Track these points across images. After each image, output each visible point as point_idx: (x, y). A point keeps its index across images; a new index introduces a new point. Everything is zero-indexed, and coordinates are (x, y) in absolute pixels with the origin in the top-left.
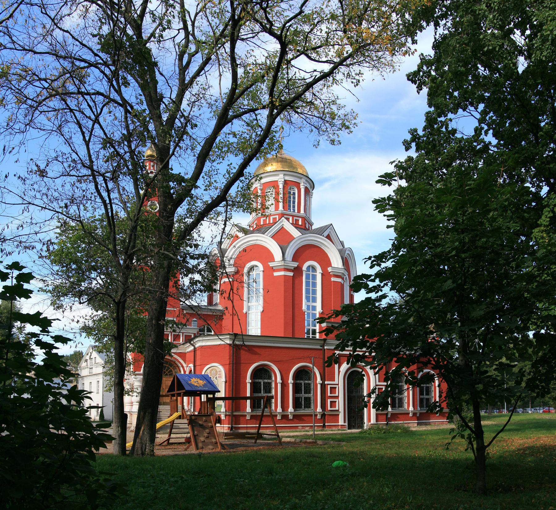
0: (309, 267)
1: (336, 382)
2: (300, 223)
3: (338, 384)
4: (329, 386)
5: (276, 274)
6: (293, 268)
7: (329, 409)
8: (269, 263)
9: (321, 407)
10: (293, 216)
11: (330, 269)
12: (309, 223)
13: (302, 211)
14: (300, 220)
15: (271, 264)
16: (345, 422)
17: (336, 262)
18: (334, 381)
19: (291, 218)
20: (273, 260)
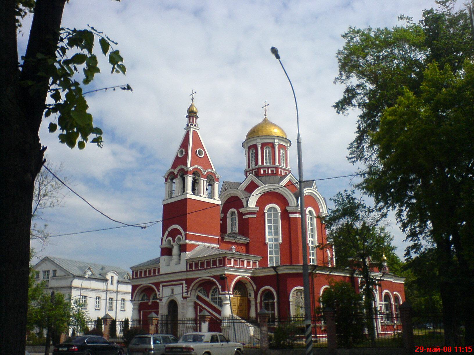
0: (271, 208)
5: (244, 217)
8: (240, 210)
14: (275, 169)
15: (241, 210)
20: (243, 207)
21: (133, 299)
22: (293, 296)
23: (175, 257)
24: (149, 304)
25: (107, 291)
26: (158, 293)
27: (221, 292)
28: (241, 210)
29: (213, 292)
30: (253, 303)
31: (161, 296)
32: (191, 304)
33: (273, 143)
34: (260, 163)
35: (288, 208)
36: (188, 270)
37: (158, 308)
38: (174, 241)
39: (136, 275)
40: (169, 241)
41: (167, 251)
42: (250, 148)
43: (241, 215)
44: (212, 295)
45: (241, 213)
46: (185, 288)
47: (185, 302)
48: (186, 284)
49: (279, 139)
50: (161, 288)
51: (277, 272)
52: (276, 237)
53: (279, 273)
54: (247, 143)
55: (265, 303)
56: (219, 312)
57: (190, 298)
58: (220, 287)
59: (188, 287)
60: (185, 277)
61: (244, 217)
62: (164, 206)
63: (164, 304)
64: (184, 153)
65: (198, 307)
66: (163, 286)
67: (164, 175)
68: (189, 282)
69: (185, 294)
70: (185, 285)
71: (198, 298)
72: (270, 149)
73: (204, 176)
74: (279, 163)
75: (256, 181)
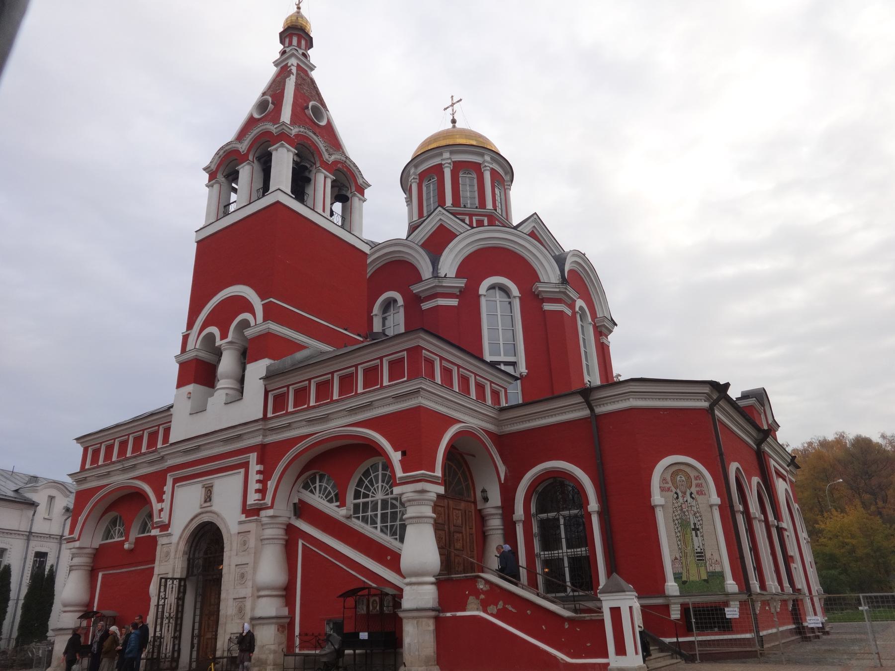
0: (492, 287)
5: (426, 306)
6: (457, 291)
10: (471, 216)
15: (416, 289)
20: (418, 279)
21: (76, 535)
22: (662, 489)
23: (224, 384)
24: (126, 546)
25: (30, 535)
26: (156, 506)
27: (399, 473)
28: (416, 289)
29: (360, 483)
30: (495, 523)
31: (165, 517)
32: (275, 532)
33: (480, 164)
35: (541, 288)
36: (270, 415)
37: (153, 561)
38: (224, 336)
39: (95, 459)
40: (211, 337)
41: (198, 372)
42: (422, 176)
43: (413, 302)
44: (357, 495)
46: (254, 477)
47: (252, 527)
48: (260, 461)
49: (492, 158)
50: (168, 488)
51: (592, 410)
53: (600, 410)
54: (416, 167)
55: (542, 524)
56: (392, 560)
57: (270, 512)
58: (396, 457)
59: (266, 475)
60: (257, 440)
61: (426, 306)
62: (198, 242)
63: (175, 539)
64: (271, 106)
65: (300, 542)
66: (176, 481)
67: (206, 163)
68: (268, 455)
69: (253, 498)
70: (254, 467)
71: (302, 510)
72: (475, 176)
73: (326, 165)
75: (452, 223)
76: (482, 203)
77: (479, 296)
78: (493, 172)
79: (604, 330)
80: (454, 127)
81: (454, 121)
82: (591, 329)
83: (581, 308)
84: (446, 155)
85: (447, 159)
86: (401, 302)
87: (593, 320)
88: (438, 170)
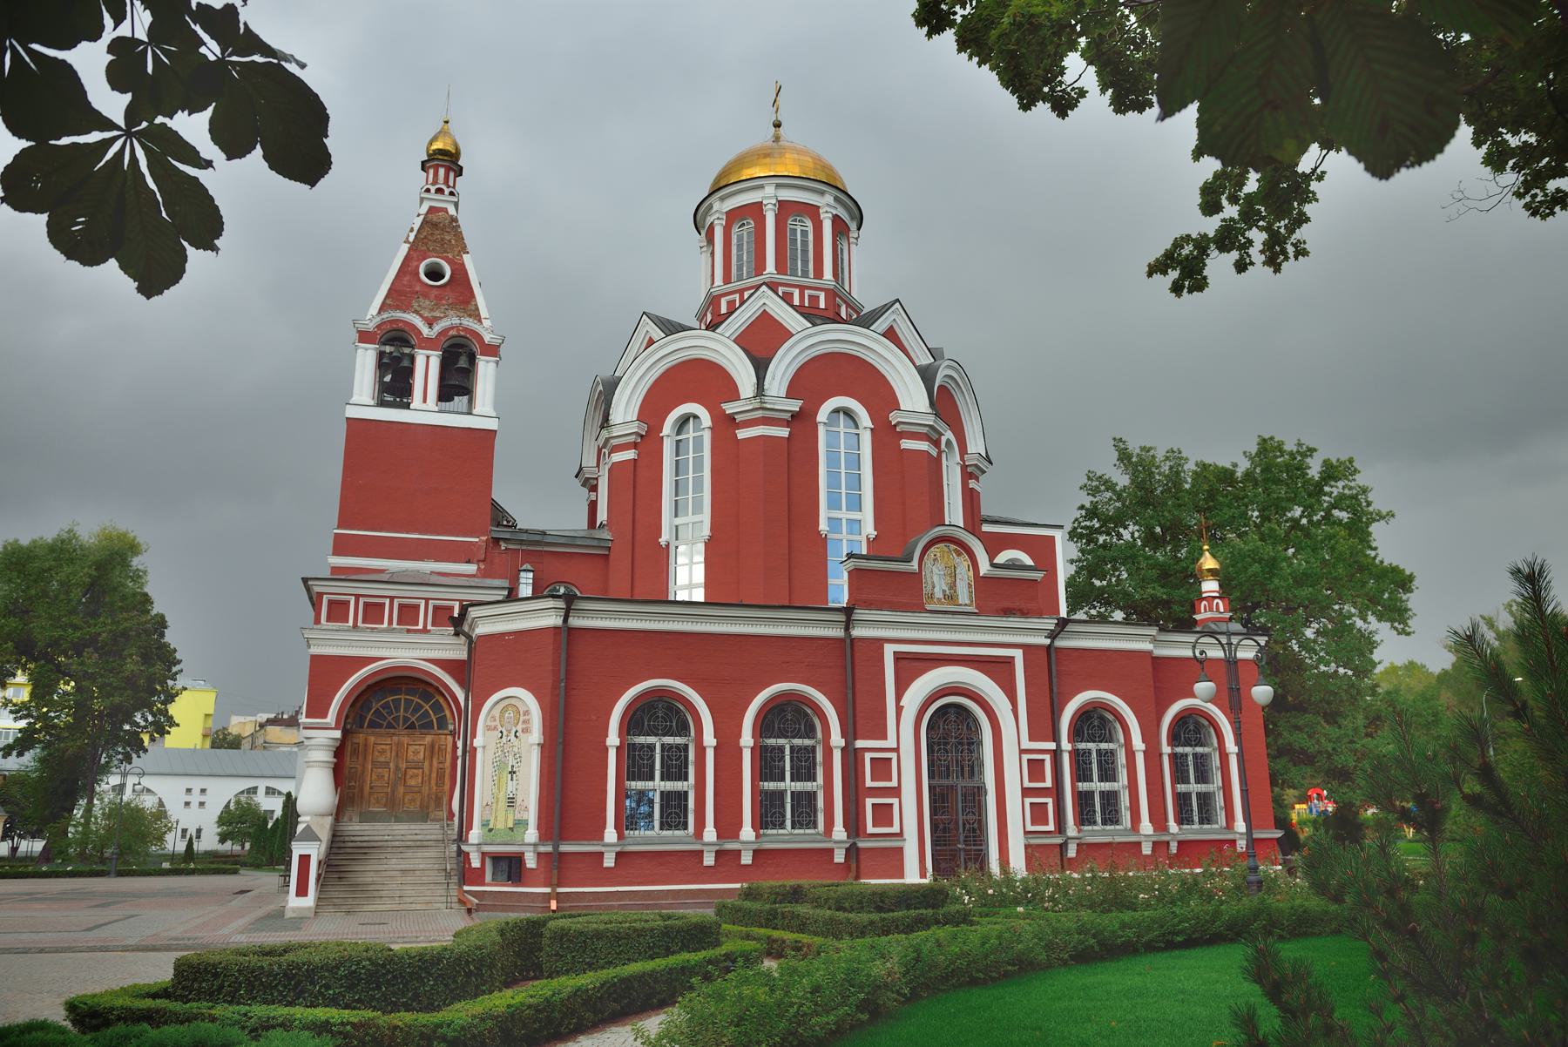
0: (837, 411)
1: (891, 742)
2: (822, 305)
3: (897, 750)
4: (868, 756)
5: (742, 434)
7: (870, 829)
8: (724, 406)
9: (845, 825)
10: (802, 288)
11: (894, 417)
12: (848, 305)
13: (828, 273)
14: (822, 296)
15: (729, 408)
16: (923, 875)
17: (913, 399)
18: (885, 737)
19: (796, 293)
20: (734, 395)
28: (729, 408)
34: (770, 266)
42: (733, 216)
43: (725, 425)
45: (731, 418)
49: (836, 199)
52: (855, 516)
72: (809, 223)
74: (835, 275)
76: (819, 273)
77: (815, 426)
78: (836, 220)
79: (978, 473)
80: (777, 139)
81: (777, 125)
82: (958, 469)
83: (948, 442)
84: (770, 190)
85: (769, 196)
86: (706, 419)
87: (962, 459)
88: (756, 210)
